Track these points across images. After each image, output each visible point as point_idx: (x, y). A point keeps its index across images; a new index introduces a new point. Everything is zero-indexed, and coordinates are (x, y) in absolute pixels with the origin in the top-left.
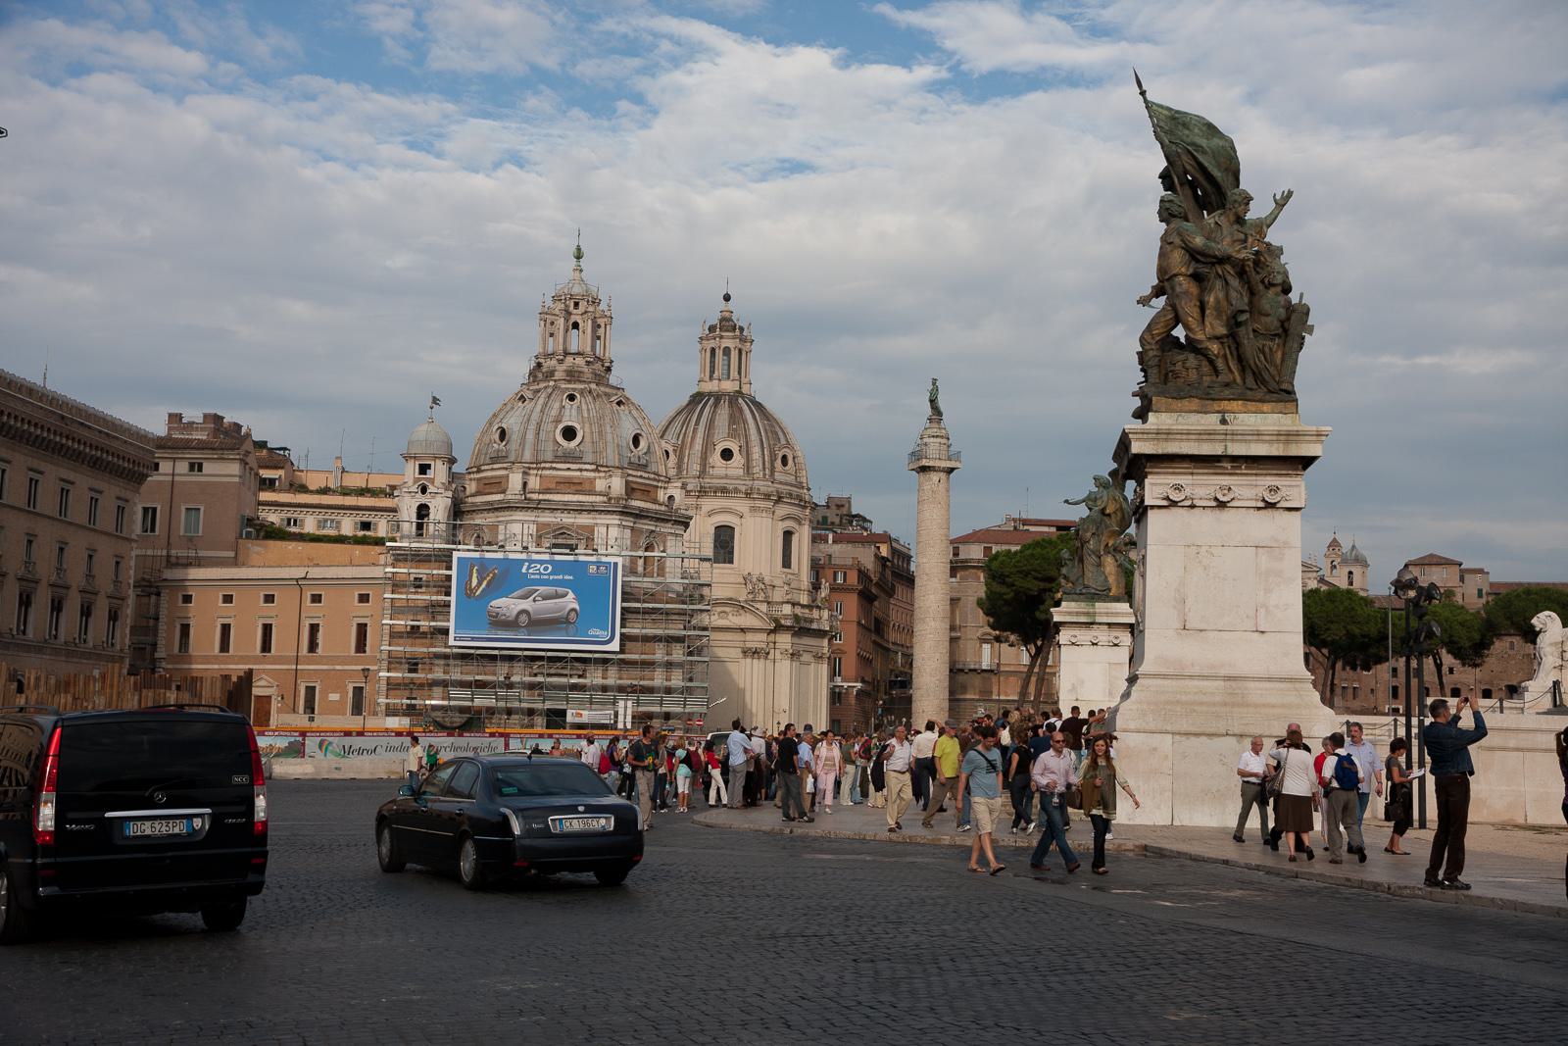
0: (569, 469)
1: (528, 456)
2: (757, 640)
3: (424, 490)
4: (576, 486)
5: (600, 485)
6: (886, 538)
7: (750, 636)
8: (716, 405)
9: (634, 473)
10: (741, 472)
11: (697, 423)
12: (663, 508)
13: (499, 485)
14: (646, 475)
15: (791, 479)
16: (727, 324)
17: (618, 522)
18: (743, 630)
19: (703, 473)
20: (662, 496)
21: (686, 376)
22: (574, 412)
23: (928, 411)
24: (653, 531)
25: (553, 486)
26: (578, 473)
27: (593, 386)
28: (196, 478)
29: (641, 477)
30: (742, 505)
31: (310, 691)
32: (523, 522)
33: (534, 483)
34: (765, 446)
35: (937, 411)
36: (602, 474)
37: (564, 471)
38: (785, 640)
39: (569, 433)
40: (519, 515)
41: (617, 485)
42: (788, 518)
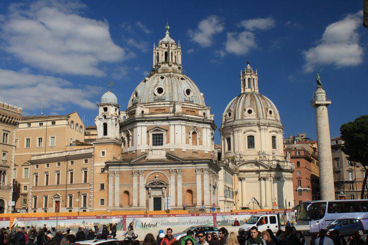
0: (160, 104)
2: (263, 174)
3: (105, 117)
4: (162, 110)
7: (261, 173)
8: (246, 96)
9: (187, 104)
12: (201, 118)
15: (274, 119)
22: (163, 83)
24: (195, 127)
25: (154, 111)
26: (163, 106)
27: (172, 73)
28: (54, 127)
29: (190, 106)
33: (146, 111)
34: (263, 107)
37: (158, 105)
39: (160, 91)
40: (139, 124)
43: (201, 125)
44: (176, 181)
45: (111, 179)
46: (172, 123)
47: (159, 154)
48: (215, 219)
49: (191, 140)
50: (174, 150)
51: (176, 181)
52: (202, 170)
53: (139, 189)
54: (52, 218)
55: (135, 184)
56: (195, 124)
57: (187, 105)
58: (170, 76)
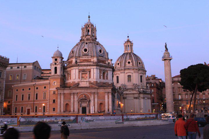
1: (77, 55)
2: (136, 96)
5: (92, 60)
6: (161, 79)
7: (135, 95)
10: (132, 66)
11: (123, 58)
12: (107, 65)
14: (103, 58)
16: (128, 41)
17: (95, 68)
18: (134, 94)
19: (125, 66)
20: (107, 62)
21: (122, 51)
22: (87, 46)
23: (165, 49)
24: (104, 70)
28: (25, 69)
30: (132, 71)
31: (36, 107)
32: (76, 69)
33: (78, 61)
35: (167, 49)
36: (92, 58)
38: (142, 95)
39: (86, 50)
40: (75, 68)
41: (95, 60)
42: (141, 73)
43: (107, 69)
44: (94, 99)
45: (59, 97)
47: (84, 84)
48: (123, 117)
49: (102, 77)
50: (93, 82)
51: (94, 99)
52: (108, 93)
53: (74, 103)
54: (39, 117)
56: (104, 69)
57: (100, 58)
58: (91, 42)
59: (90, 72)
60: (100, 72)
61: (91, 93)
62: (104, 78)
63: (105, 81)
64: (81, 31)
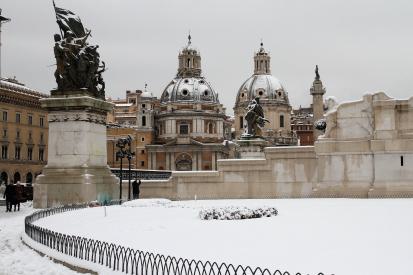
13: (165, 109)
23: (315, 75)
43: (215, 119)
45: (149, 158)
46: (195, 117)
47: (184, 140)
55: (168, 161)
57: (206, 103)
59: (191, 124)
60: (206, 123)
61: (192, 153)
62: (211, 132)
63: (212, 136)
64: (178, 60)
